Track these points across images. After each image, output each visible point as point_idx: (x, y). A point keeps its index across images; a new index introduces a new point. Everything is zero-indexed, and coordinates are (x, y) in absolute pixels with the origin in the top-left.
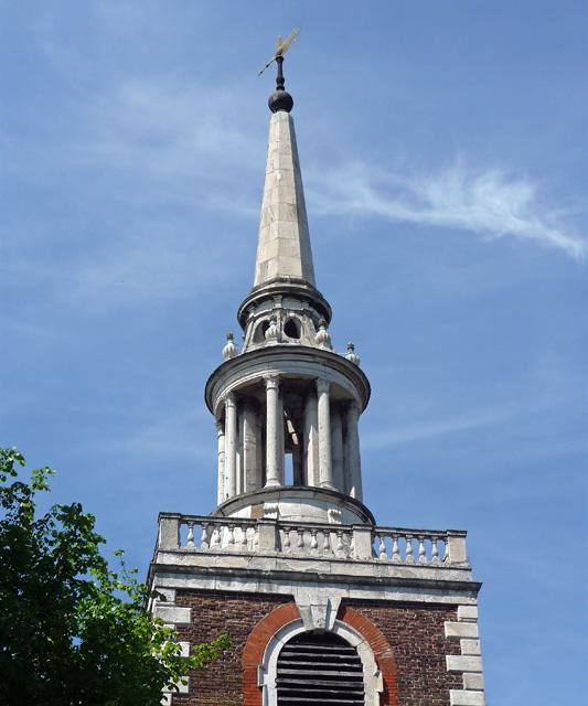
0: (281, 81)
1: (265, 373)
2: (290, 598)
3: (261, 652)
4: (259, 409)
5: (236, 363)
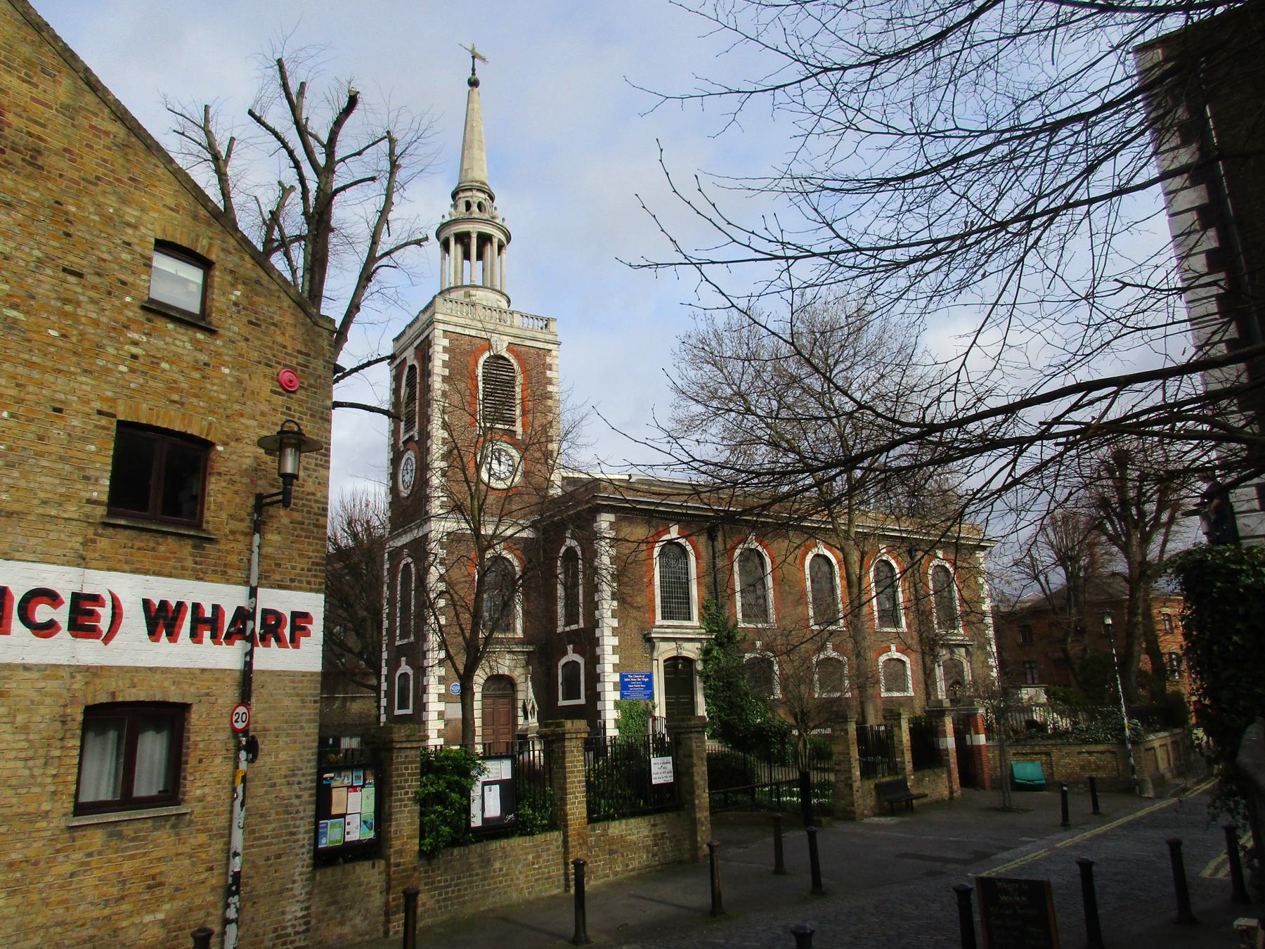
0: (473, 70)
5: (455, 222)
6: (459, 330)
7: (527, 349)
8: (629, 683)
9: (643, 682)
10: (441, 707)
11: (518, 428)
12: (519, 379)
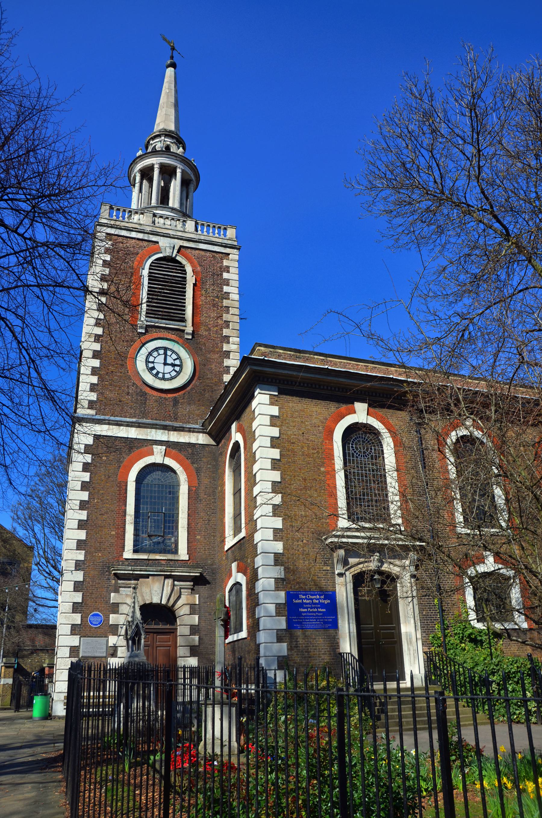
1: (154, 162)
2: (158, 243)
3: (141, 265)
4: (151, 180)
6: (124, 233)
7: (203, 253)
8: (302, 605)
9: (323, 606)
10: (75, 641)
11: (189, 329)
12: (190, 279)
